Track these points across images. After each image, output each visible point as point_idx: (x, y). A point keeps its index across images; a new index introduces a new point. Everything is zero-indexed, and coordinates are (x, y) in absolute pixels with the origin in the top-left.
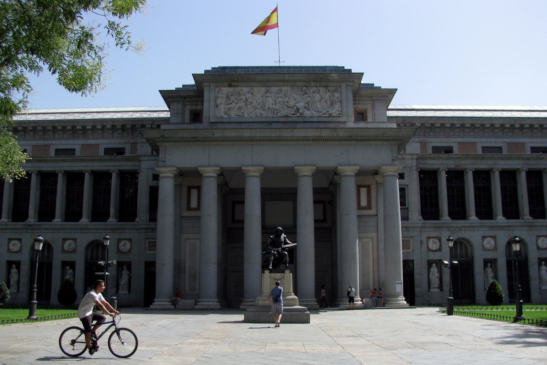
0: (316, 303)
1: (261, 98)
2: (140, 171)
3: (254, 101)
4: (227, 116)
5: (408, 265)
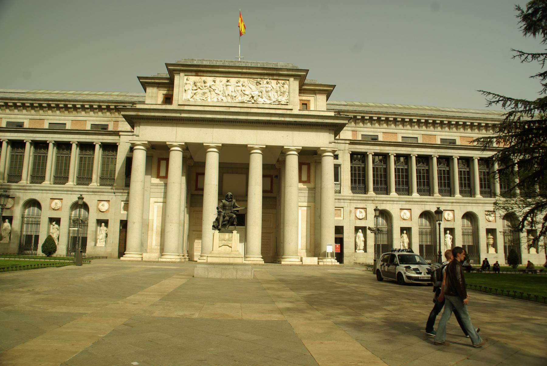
0: (262, 260)
1: (222, 86)
2: (119, 144)
3: (216, 88)
4: (193, 100)
5: (339, 230)
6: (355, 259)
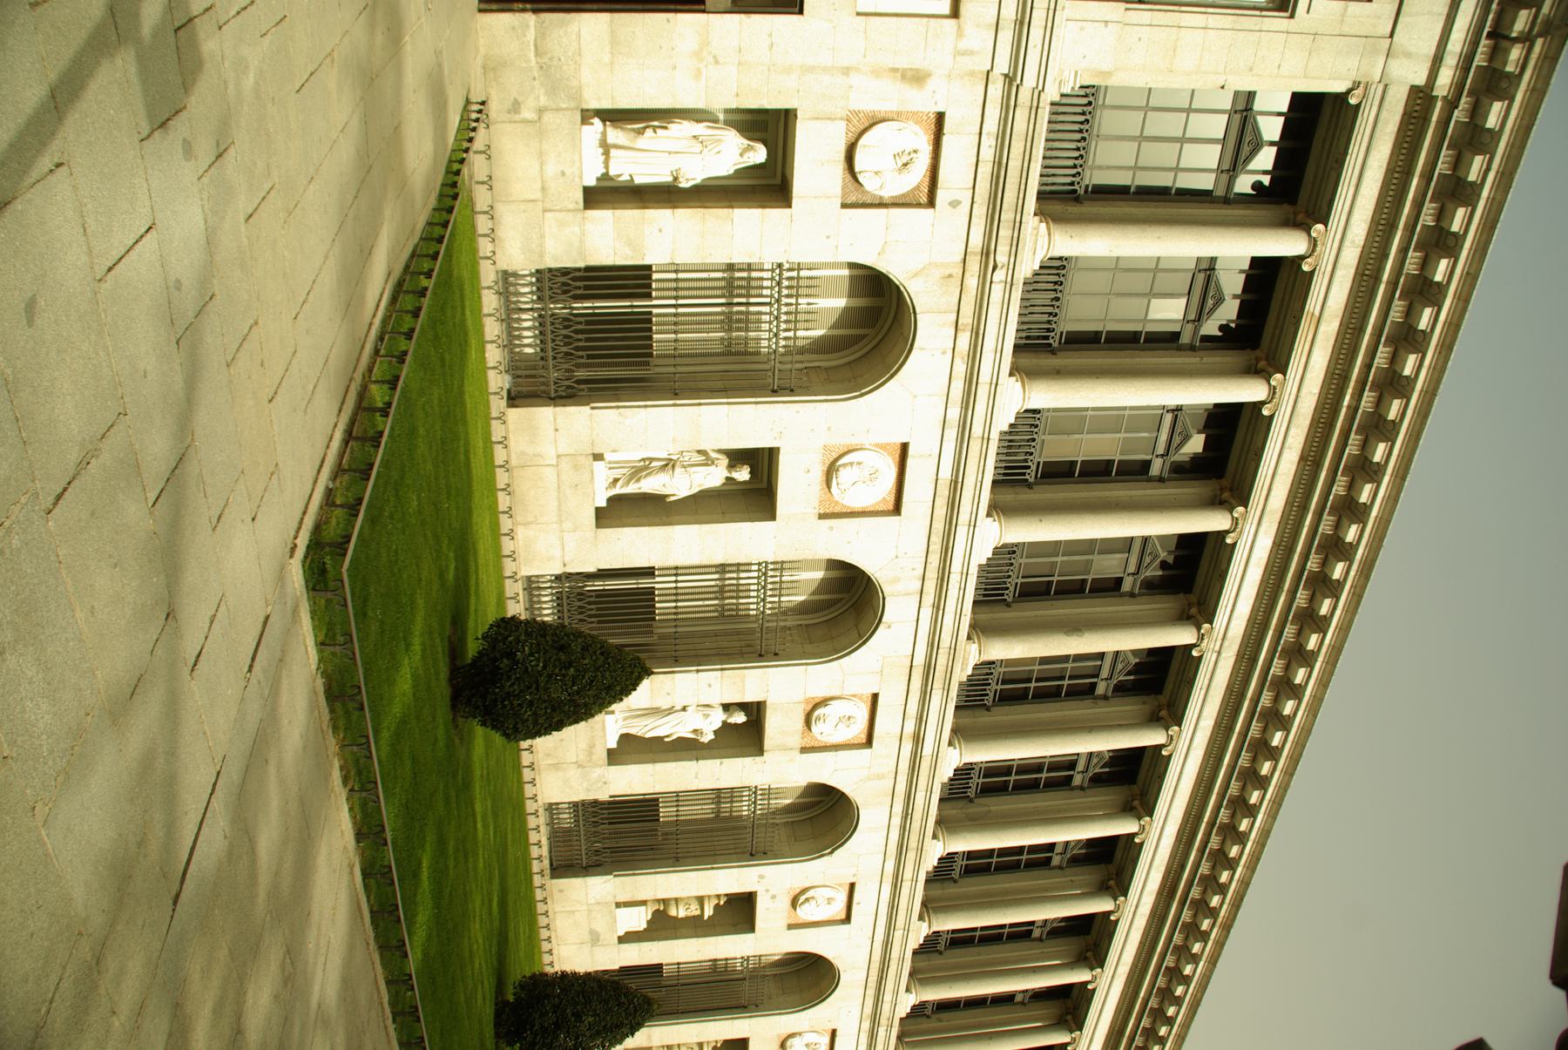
6: (528, 114)
